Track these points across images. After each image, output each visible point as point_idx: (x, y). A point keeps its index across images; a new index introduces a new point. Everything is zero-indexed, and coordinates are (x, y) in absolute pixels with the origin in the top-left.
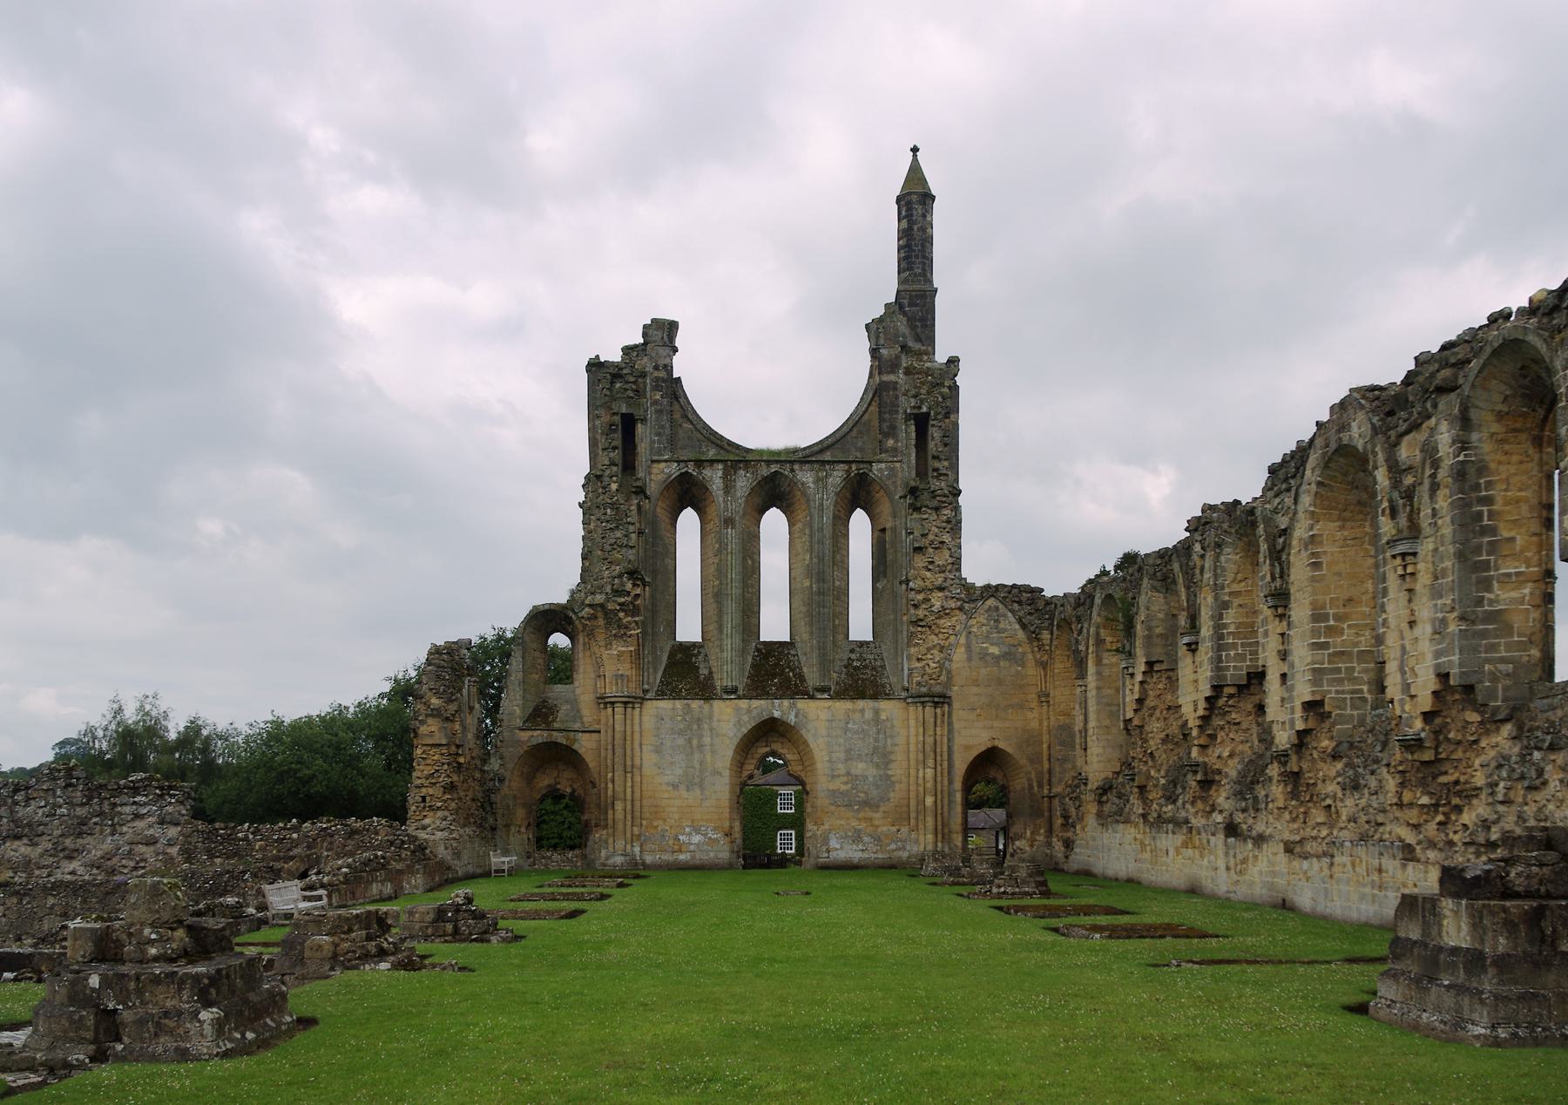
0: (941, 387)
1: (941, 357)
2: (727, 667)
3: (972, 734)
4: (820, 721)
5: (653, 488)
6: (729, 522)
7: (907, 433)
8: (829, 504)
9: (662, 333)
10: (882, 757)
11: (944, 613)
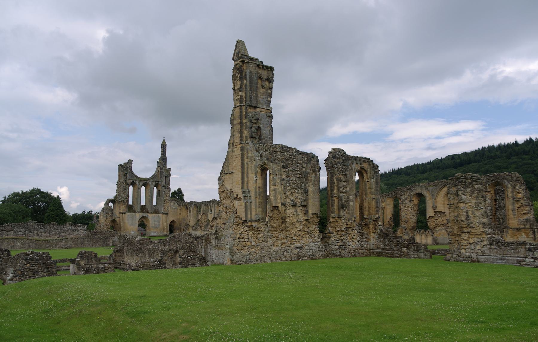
1: (168, 167)
2: (138, 209)
3: (171, 219)
4: (151, 217)
9: (130, 162)
10: (159, 221)
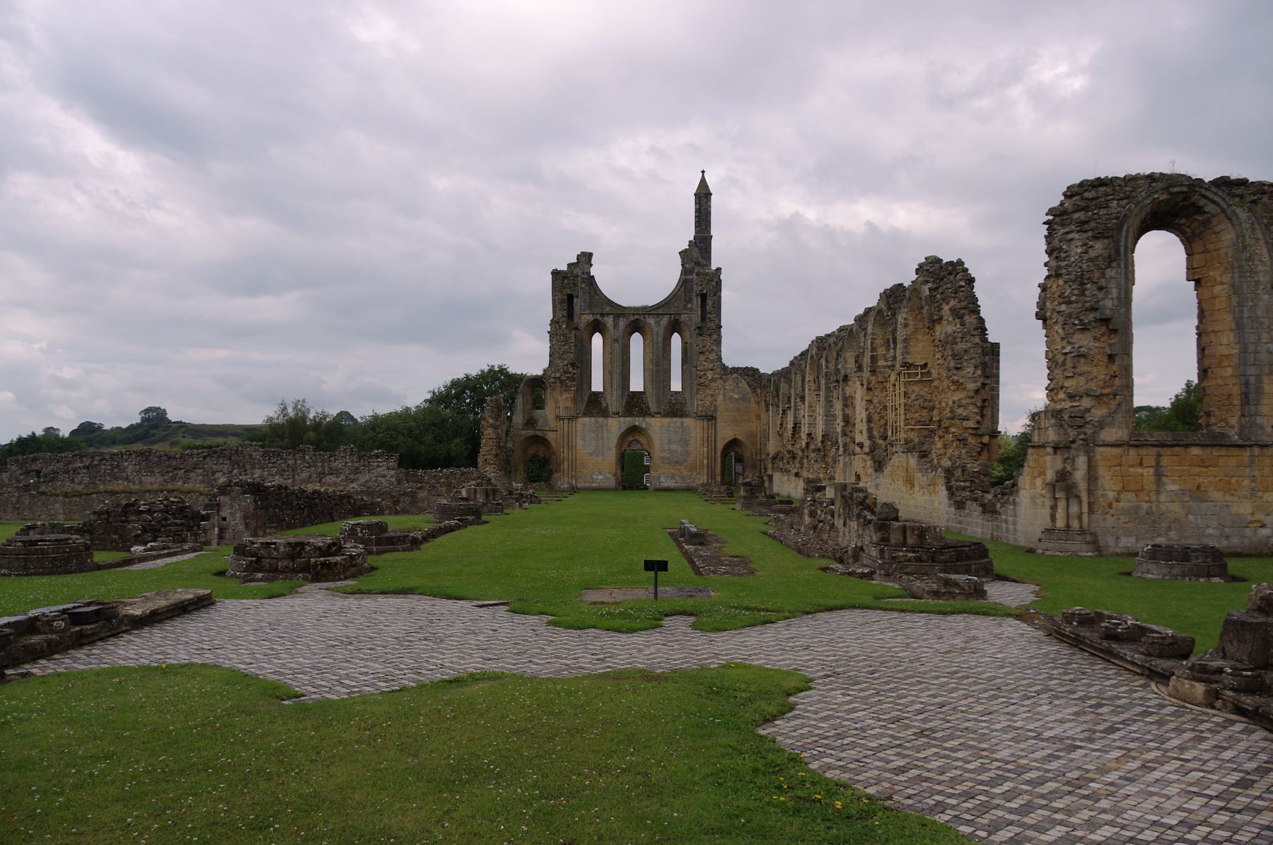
0: (714, 281)
1: (714, 267)
2: (614, 402)
3: (725, 433)
4: (657, 427)
5: (582, 326)
6: (616, 340)
7: (697, 302)
8: (661, 332)
9: (586, 258)
10: (685, 442)
11: (713, 380)
